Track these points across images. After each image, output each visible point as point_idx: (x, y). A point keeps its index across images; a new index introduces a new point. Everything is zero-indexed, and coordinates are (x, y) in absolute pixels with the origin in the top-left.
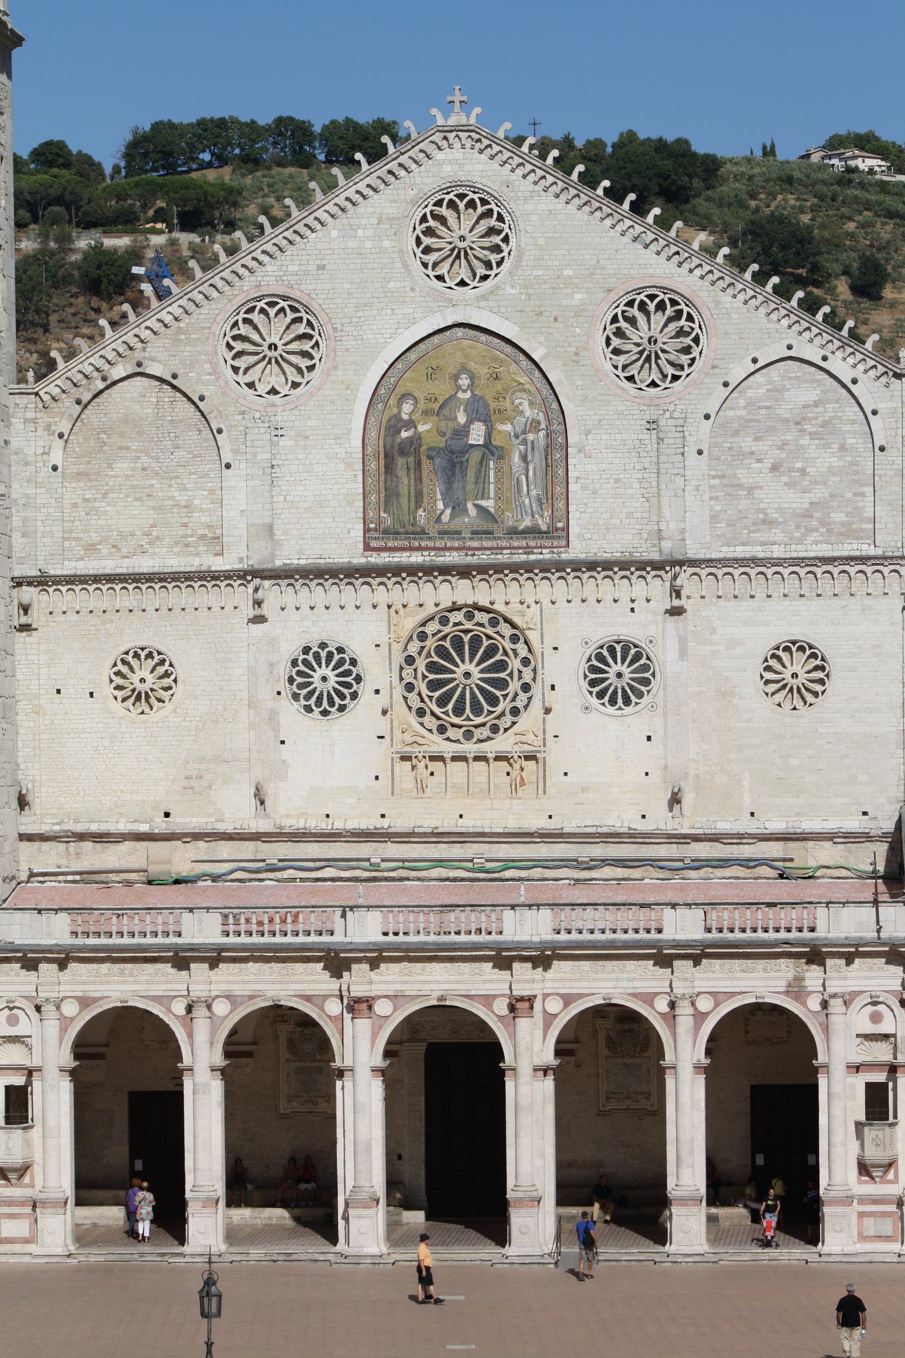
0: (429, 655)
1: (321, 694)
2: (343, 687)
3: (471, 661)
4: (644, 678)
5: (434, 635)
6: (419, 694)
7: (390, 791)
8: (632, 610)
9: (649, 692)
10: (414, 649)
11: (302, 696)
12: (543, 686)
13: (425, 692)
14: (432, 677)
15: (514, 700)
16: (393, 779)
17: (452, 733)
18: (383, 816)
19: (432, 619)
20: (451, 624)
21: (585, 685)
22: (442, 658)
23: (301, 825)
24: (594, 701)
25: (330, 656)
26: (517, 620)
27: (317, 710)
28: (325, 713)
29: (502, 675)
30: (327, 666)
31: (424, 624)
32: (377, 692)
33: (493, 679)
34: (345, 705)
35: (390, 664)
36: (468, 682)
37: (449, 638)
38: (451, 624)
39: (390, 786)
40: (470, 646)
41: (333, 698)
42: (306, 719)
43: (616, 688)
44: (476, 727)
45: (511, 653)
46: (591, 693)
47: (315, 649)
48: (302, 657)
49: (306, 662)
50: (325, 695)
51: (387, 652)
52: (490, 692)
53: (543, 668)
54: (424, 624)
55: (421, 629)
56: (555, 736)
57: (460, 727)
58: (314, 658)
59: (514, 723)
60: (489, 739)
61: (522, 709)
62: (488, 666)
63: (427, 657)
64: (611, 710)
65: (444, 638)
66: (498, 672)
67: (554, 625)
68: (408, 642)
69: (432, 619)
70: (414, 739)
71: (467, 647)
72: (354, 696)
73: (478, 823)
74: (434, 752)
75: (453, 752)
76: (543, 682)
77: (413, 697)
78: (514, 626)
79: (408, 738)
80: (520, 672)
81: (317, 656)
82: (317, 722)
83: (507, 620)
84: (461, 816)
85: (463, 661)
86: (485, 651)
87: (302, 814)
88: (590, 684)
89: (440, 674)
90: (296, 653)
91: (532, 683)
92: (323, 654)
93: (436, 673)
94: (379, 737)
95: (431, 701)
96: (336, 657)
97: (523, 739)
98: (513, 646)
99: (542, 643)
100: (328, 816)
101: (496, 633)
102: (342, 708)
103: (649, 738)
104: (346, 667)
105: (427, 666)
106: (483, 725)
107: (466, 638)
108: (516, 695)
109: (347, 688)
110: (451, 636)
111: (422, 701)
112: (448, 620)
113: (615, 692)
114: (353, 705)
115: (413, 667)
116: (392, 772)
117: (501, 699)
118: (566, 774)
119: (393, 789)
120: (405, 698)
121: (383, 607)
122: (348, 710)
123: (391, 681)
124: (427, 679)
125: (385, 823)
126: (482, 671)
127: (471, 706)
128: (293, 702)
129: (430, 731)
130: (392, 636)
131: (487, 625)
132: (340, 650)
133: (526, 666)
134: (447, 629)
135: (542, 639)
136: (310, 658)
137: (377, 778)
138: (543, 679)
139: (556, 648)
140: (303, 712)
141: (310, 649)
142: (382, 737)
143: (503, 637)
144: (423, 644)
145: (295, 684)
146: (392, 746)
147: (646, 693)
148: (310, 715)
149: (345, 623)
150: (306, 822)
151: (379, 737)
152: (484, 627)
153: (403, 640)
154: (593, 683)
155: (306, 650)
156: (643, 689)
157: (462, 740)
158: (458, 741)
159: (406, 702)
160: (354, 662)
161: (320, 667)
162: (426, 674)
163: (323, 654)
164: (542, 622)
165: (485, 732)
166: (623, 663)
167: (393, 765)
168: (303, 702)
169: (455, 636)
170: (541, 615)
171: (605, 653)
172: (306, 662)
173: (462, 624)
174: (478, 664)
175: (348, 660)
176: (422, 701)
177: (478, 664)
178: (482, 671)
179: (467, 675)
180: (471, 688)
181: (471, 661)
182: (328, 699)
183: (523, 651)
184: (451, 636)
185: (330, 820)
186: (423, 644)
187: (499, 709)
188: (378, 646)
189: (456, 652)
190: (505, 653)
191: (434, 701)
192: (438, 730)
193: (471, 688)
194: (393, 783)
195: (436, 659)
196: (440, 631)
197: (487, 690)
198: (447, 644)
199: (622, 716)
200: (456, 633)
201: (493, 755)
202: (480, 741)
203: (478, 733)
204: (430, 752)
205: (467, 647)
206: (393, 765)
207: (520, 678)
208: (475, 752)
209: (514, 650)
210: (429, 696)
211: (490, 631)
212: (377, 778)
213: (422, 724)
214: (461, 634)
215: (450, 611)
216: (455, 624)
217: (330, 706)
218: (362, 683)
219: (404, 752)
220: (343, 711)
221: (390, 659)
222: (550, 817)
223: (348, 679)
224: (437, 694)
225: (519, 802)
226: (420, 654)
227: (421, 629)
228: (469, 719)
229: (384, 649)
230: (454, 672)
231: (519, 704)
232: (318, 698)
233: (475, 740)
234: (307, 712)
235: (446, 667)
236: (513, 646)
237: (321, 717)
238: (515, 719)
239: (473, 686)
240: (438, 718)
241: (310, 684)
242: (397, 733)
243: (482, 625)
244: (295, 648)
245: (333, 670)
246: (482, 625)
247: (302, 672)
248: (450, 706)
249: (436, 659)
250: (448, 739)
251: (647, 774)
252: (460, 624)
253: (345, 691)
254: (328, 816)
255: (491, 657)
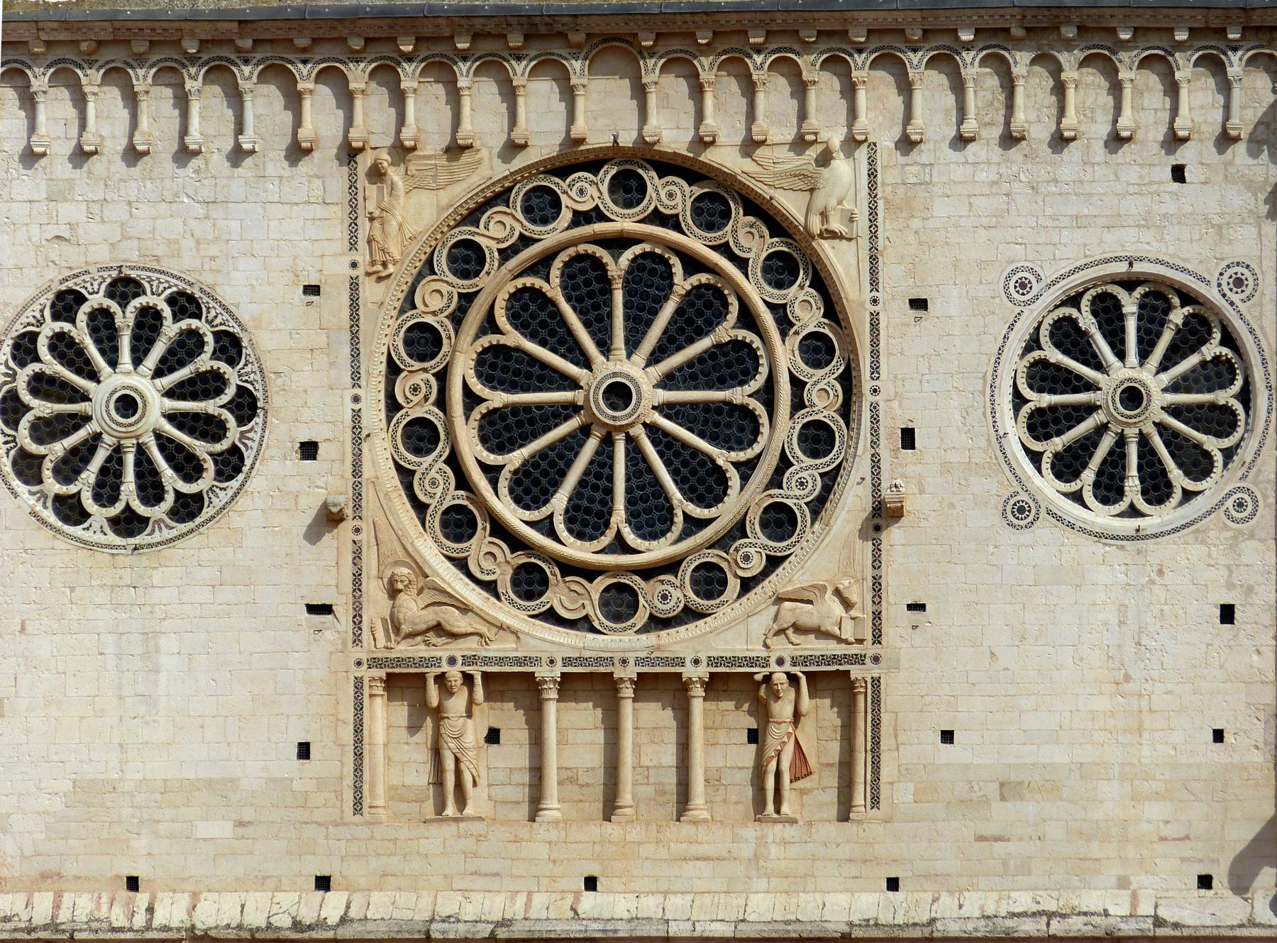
0: (490, 325)
1: (117, 455)
2: (191, 432)
3: (633, 344)
4: (1213, 406)
5: (505, 255)
6: (454, 461)
7: (349, 796)
8: (1178, 173)
9: (1228, 454)
10: (436, 303)
11: (48, 465)
12: (875, 432)
13: (472, 449)
14: (498, 399)
15: (776, 481)
16: (359, 755)
17: (559, 596)
18: (323, 883)
19: (502, 197)
20: (566, 216)
21: (1015, 431)
22: (533, 336)
23: (41, 910)
24: (1047, 487)
25: (148, 323)
26: (791, 204)
27: (99, 514)
28: (128, 524)
29: (738, 395)
30: (137, 361)
31: (472, 216)
32: (309, 450)
33: (707, 406)
34: (198, 498)
35: (355, 354)
36: (621, 417)
37: (558, 264)
38: (566, 216)
39: (349, 780)
40: (629, 293)
41: (155, 473)
42: (61, 544)
43: (1121, 441)
44: (648, 572)
45: (768, 319)
46: (1035, 458)
47: (98, 300)
48: (51, 327)
49: (64, 347)
50: (130, 459)
51: (346, 312)
52: (696, 452)
53: (875, 369)
54: (472, 216)
55: (464, 233)
56: (912, 607)
57: (590, 573)
58: (94, 331)
59: (774, 562)
60: (690, 615)
61: (802, 515)
62: (690, 364)
63: (482, 331)
64: (1101, 516)
65: (541, 266)
66: (722, 383)
67: (916, 223)
68: (420, 277)
69: (502, 197)
70: (431, 616)
71: (618, 297)
72: (231, 464)
73: (650, 906)
74: (501, 661)
75: (567, 661)
76: (875, 420)
77: (432, 466)
78: (776, 224)
79: (413, 609)
80: (797, 384)
81: (103, 325)
82: (103, 557)
83: (758, 209)
84: (591, 883)
85: (605, 346)
86: (679, 312)
87: (45, 876)
88: (1031, 428)
89: (526, 389)
90: (28, 317)
91: (837, 424)
92: (125, 319)
93: (513, 387)
94: (313, 609)
95: (494, 483)
96: (171, 329)
97: (807, 615)
98: (776, 296)
99: (874, 283)
100: (133, 883)
101: (724, 249)
102: (188, 508)
103: (1227, 614)
104: (205, 362)
105: (480, 362)
106: (672, 566)
107: (618, 266)
108: (785, 462)
109: (204, 436)
110: (564, 257)
111: (463, 482)
112: (556, 204)
113: (1117, 456)
114: (224, 496)
115: (436, 364)
116: (358, 729)
117: (734, 476)
118: (948, 736)
119: (358, 790)
120: (406, 475)
121: (326, 156)
122: (206, 513)
123: (357, 415)
124: (483, 408)
125: (332, 906)
126: (668, 381)
127: (630, 502)
128: (17, 483)
129: (490, 587)
130: (362, 256)
131: (687, 220)
132: (185, 304)
133: (817, 364)
134: (553, 234)
135: (874, 272)
136: (80, 332)
137: (304, 751)
138: (874, 408)
139: (919, 304)
140: (52, 518)
141: (81, 299)
142: (325, 609)
143: (742, 264)
144: (466, 286)
145: (25, 423)
146: (357, 640)
147: (1218, 458)
148: (77, 531)
149: (200, 210)
150: (57, 906)
151: (313, 609)
152: (677, 227)
153: (402, 274)
154: (1042, 424)
155: (67, 303)
156: (1212, 444)
157: (599, 619)
158: (583, 624)
159: (409, 489)
160: (230, 347)
161: (113, 363)
162: (478, 388)
163: (125, 319)
164: (873, 213)
165: (679, 592)
166: (1144, 355)
167: (359, 707)
168: (52, 486)
169: (579, 258)
170: (872, 187)
171: (1087, 321)
172: (64, 347)
173: (602, 218)
174: (654, 359)
175: (209, 339)
176: (463, 482)
177: (654, 359)
178: (668, 381)
179: (619, 394)
180: (630, 440)
181: (633, 344)
182: (139, 475)
183: (809, 318)
184: (564, 257)
185: (142, 899)
186: (466, 286)
187: (725, 513)
188: (312, 290)
189: (580, 312)
190: (748, 319)
191: (503, 484)
192: (515, 583)
193: (630, 440)
194: (358, 769)
195: (513, 338)
196: (525, 241)
197: (685, 445)
198: (553, 288)
199: (1138, 536)
200: (582, 248)
201: (703, 671)
202: (658, 623)
203: (650, 595)
204: (487, 661)
205: (618, 297)
206: (359, 707)
207: (798, 404)
208: (638, 661)
209: (780, 311)
210: (485, 468)
211: (697, 243)
212: (304, 751)
213: (461, 564)
214: (600, 252)
215: (562, 170)
216: (580, 218)
217: (146, 501)
218: (258, 420)
219: (400, 661)
220: (192, 516)
221: (355, 337)
222: (893, 884)
223: (211, 406)
224: (516, 458)
225: (789, 831)
226: (457, 319)
227: (464, 233)
228: (620, 545)
229: (336, 301)
230: (573, 384)
231: (794, 496)
232: (104, 471)
233: (641, 618)
234: (66, 519)
235: (544, 366)
236: (776, 296)
237: (113, 538)
238: (778, 547)
239: (639, 431)
240: (516, 543)
241: (81, 420)
242: (374, 591)
243: (672, 222)
244: (22, 296)
245: (158, 373)
246: (672, 222)
247: (52, 380)
248: (559, 501)
249: (513, 338)
250: (551, 616)
251: (1218, 736)
252: (598, 215)
253: (201, 448)
254: (133, 883)
255: (700, 333)
